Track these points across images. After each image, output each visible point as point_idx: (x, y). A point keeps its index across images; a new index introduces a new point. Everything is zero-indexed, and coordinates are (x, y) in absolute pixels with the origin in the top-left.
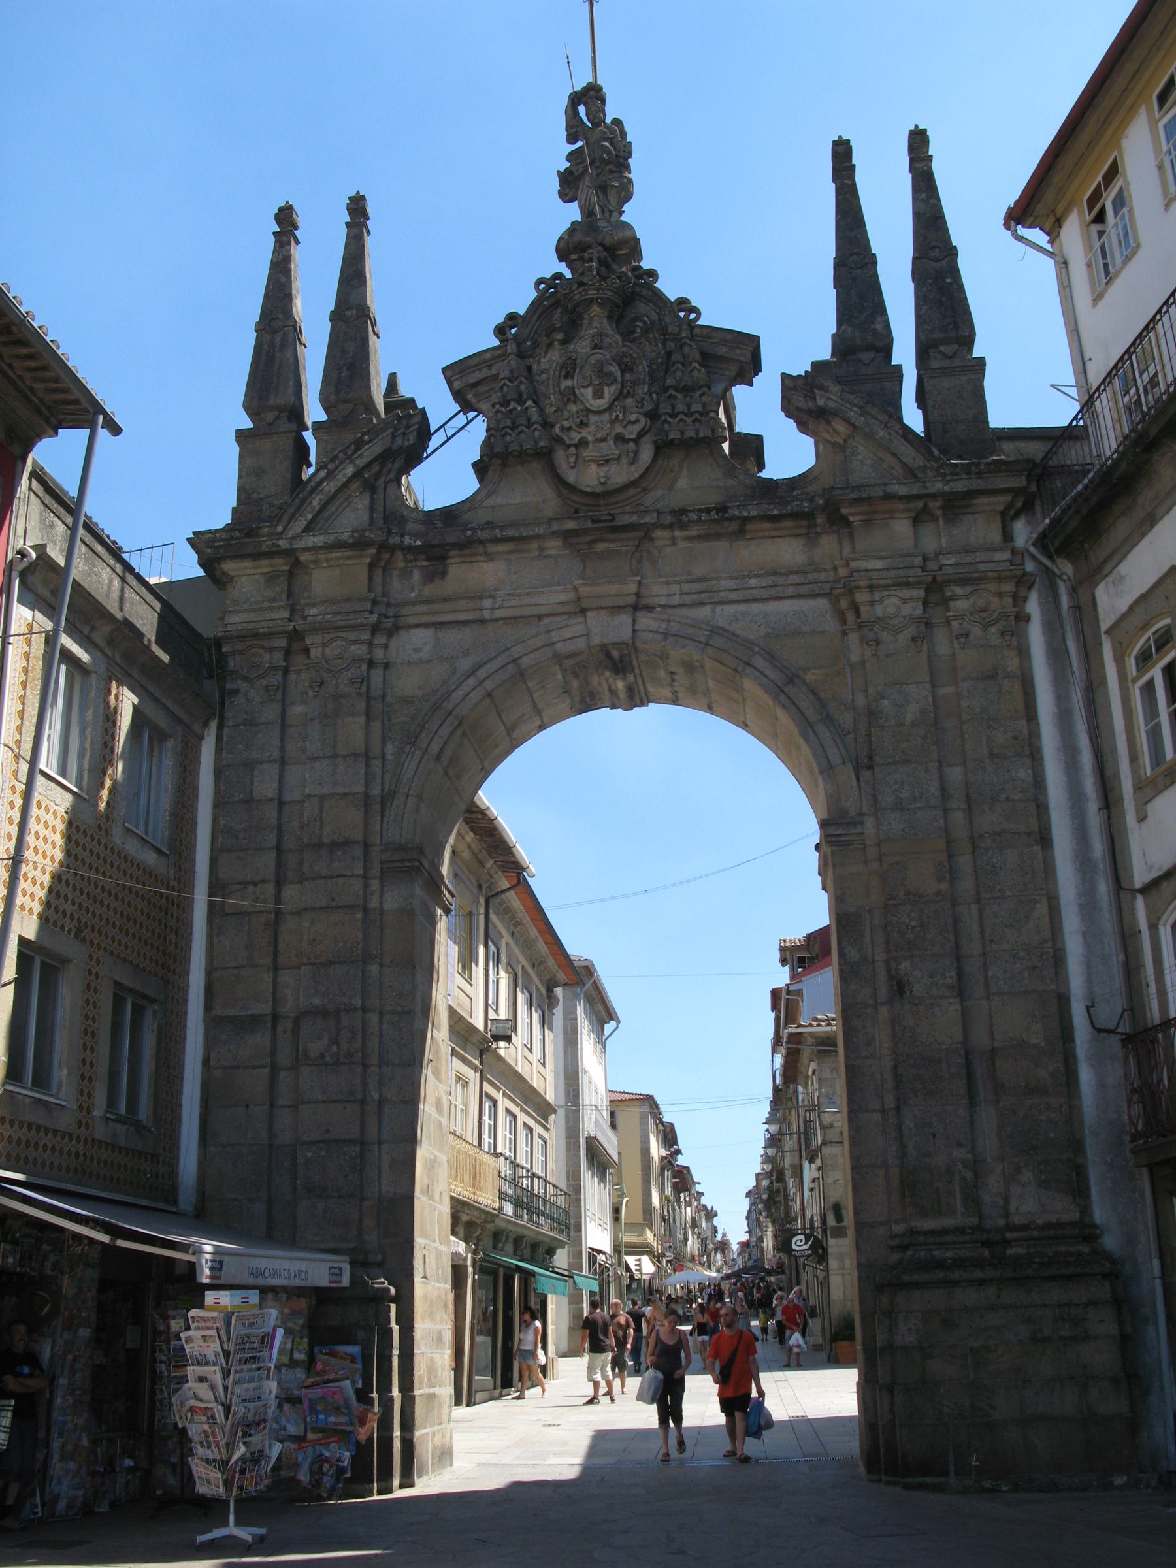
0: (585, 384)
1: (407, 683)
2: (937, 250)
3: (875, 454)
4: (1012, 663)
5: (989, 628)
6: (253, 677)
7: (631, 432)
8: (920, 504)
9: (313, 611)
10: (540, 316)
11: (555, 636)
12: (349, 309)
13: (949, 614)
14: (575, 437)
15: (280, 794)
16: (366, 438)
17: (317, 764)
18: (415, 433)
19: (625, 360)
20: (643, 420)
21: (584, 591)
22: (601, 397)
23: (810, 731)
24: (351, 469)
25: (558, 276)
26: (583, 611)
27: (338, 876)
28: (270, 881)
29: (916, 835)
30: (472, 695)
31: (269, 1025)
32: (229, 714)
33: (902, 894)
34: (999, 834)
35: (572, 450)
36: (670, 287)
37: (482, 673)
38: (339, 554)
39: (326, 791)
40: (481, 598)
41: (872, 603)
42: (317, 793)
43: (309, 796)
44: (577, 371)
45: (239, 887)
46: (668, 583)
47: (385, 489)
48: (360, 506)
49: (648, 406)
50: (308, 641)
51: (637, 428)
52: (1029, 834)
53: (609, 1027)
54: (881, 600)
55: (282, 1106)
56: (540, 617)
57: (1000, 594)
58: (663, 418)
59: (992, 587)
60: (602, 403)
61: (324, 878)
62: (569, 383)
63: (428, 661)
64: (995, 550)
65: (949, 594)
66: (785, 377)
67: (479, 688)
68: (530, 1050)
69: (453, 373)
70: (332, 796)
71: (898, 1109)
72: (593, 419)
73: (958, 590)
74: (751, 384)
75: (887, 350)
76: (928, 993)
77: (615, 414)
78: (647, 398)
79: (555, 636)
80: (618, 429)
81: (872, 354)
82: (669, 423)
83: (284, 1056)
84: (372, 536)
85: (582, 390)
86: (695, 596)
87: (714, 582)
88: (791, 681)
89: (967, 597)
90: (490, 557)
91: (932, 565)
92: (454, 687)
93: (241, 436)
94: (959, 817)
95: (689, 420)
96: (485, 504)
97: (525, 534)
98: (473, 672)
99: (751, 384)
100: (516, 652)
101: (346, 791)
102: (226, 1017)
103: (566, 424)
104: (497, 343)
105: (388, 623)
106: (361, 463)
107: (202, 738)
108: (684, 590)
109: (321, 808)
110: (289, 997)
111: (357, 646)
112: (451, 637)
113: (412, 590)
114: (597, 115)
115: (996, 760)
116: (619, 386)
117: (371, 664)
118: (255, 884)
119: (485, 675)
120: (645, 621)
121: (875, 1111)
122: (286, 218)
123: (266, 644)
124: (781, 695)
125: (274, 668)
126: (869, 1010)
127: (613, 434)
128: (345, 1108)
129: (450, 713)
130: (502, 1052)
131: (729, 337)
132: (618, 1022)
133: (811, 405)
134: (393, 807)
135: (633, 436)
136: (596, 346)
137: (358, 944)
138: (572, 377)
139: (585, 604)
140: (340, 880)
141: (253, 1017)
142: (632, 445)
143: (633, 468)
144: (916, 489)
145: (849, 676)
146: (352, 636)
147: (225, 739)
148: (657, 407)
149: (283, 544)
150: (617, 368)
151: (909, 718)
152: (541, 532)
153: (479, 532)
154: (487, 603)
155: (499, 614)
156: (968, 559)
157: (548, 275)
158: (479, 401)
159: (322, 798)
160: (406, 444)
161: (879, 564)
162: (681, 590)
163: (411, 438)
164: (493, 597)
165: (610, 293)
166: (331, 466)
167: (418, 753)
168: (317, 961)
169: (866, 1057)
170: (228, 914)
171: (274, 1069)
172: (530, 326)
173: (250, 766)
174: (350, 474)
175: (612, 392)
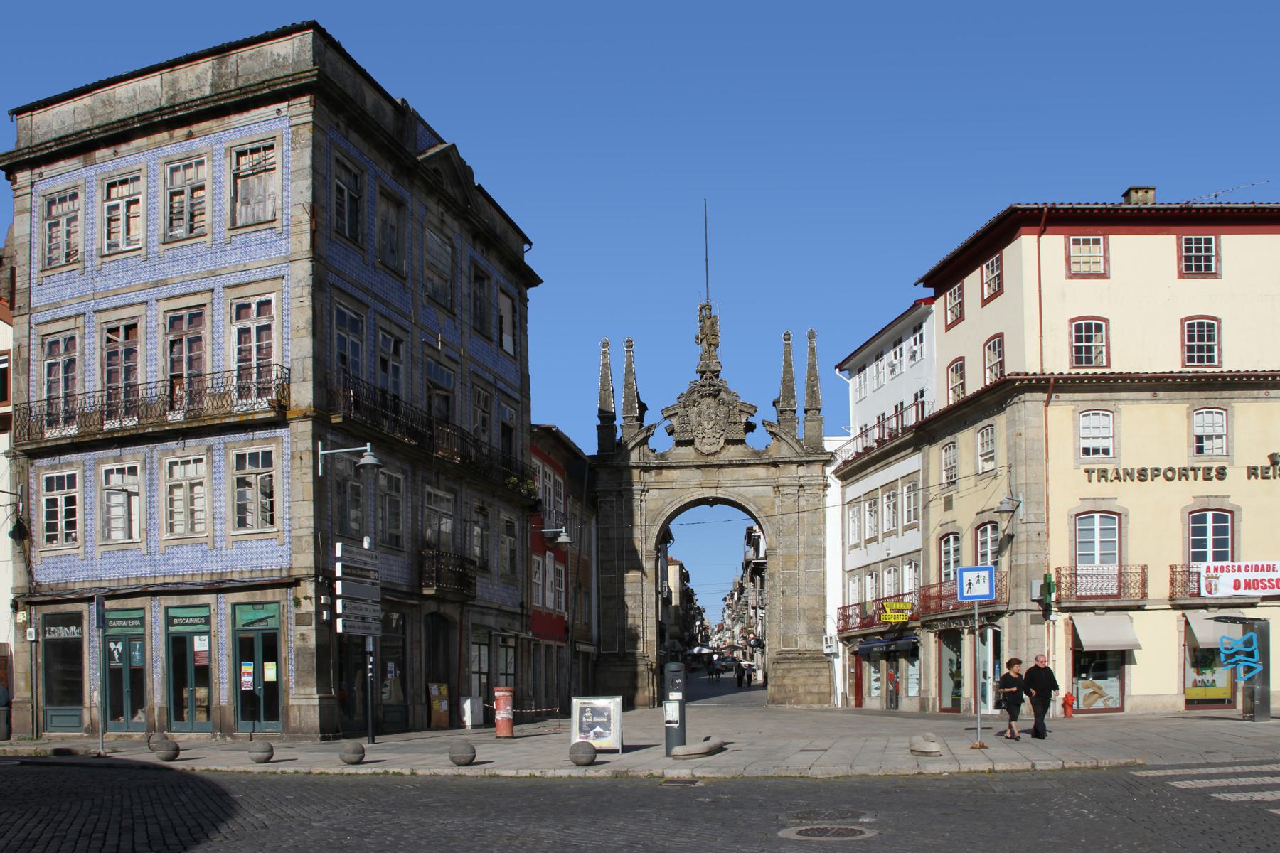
1: (651, 505)
7: (718, 435)
14: (701, 436)
37: (673, 504)
60: (710, 427)
72: (707, 431)
80: (714, 434)
88: (760, 510)
91: (801, 479)
93: (598, 426)
100: (682, 498)
105: (646, 489)
106: (637, 441)
112: (663, 492)
117: (641, 501)
120: (719, 491)
144: (798, 459)
157: (693, 380)
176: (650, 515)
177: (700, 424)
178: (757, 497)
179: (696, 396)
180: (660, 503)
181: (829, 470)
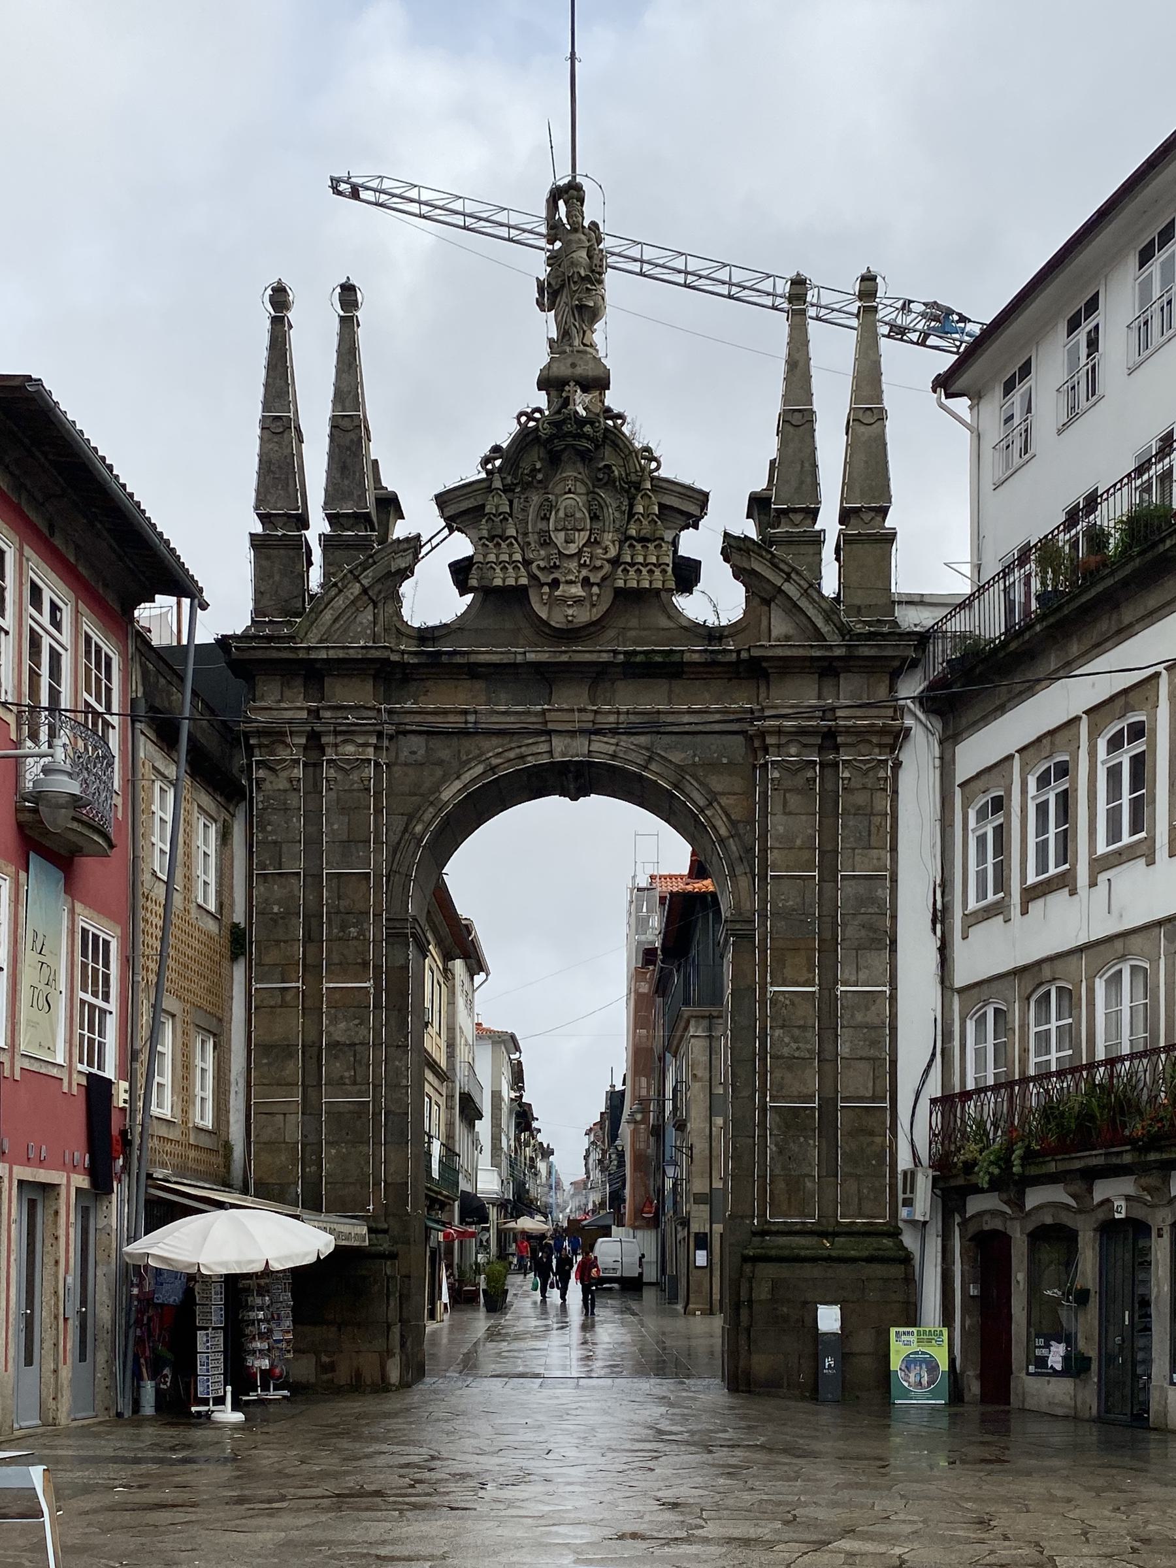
8: (826, 664)
20: (607, 567)
35: (546, 589)
51: (601, 574)
57: (880, 745)
59: (875, 740)
60: (573, 549)
69: (442, 500)
73: (849, 740)
75: (813, 514)
80: (584, 572)
103: (542, 564)
114: (575, 210)
116: (588, 533)
122: (280, 298)
127: (581, 578)
135: (598, 581)
138: (548, 519)
142: (595, 590)
148: (619, 555)
179: (535, 459)
181: (911, 687)
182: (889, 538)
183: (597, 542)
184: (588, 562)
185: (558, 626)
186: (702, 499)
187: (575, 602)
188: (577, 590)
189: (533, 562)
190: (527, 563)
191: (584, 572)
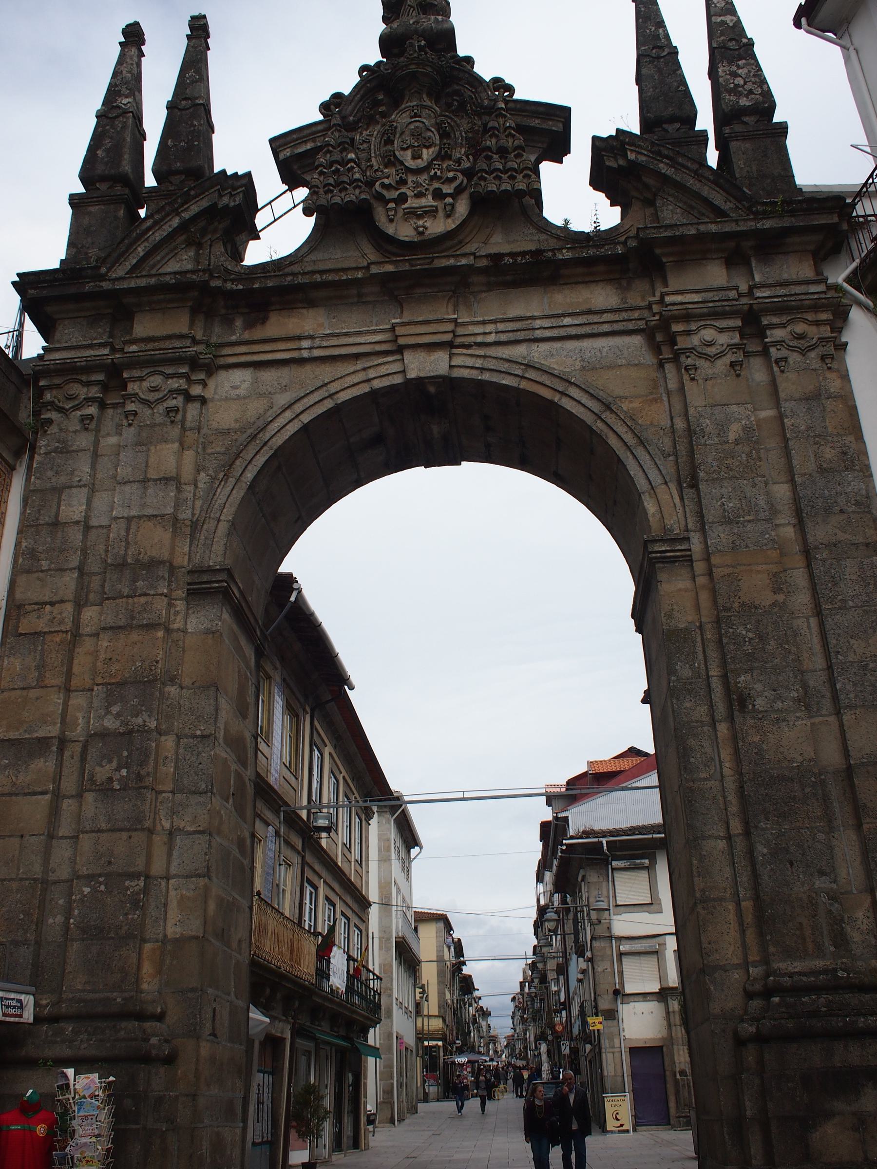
0: (405, 146)
2: (734, 42)
3: (685, 203)
4: (834, 384)
5: (809, 354)
6: (67, 407)
9: (134, 348)
10: (362, 97)
11: (372, 374)
12: (186, 99)
13: (766, 340)
14: (395, 194)
15: (87, 517)
16: (192, 193)
17: (127, 488)
18: (241, 195)
19: (443, 126)
20: (460, 176)
21: (399, 331)
22: (420, 157)
23: (629, 454)
24: (177, 221)
25: (381, 62)
26: (401, 350)
27: (140, 595)
28: (69, 601)
29: (747, 546)
30: (287, 427)
31: (54, 748)
32: (42, 443)
33: (736, 605)
34: (835, 545)
35: (392, 205)
36: (485, 70)
37: (298, 407)
38: (162, 297)
39: (134, 513)
40: (300, 338)
41: (688, 333)
42: (125, 515)
43: (116, 518)
44: (398, 135)
45: (36, 607)
46: (484, 323)
47: (211, 246)
48: (186, 257)
49: (466, 165)
50: (125, 375)
52: (867, 545)
53: (414, 851)
54: (698, 329)
55: (62, 838)
56: (357, 356)
57: (817, 323)
58: (479, 175)
59: (810, 317)
60: (420, 164)
61: (127, 597)
62: (389, 147)
63: (245, 398)
64: (808, 282)
65: (765, 322)
66: (595, 139)
67: (296, 421)
68: (349, 850)
69: (277, 144)
70: (140, 517)
71: (747, 833)
73: (775, 320)
74: (561, 162)
76: (771, 707)
77: (433, 172)
78: (464, 158)
79: (372, 374)
80: (436, 185)
81: (677, 125)
82: (485, 179)
83: (69, 785)
84: (194, 277)
85: (402, 153)
86: (511, 334)
87: (530, 321)
89: (783, 326)
90: (312, 304)
92: (271, 419)
94: (789, 532)
95: (505, 177)
96: (306, 259)
97: (345, 277)
98: (290, 406)
99: (561, 162)
100: (333, 387)
101: (155, 513)
102: (9, 740)
103: (386, 181)
104: (321, 117)
106: (186, 215)
107: (13, 468)
108: (500, 330)
109: (128, 530)
110: (80, 721)
111: (175, 379)
112: (269, 376)
113: (235, 334)
115: (825, 475)
116: (437, 148)
118: (52, 604)
119: (302, 409)
121: (718, 837)
123: (84, 378)
124: (599, 421)
125: (89, 400)
126: (706, 729)
127: (431, 189)
128: (130, 837)
129: (266, 443)
130: (324, 843)
131: (541, 109)
132: (421, 848)
133: (621, 162)
134: (204, 532)
135: (450, 191)
136: (416, 115)
137: (157, 662)
139: (402, 341)
140: (143, 600)
141: (39, 740)
142: (449, 200)
143: (450, 221)
145: (666, 404)
146: (169, 370)
147: (35, 466)
149: (106, 285)
150: (436, 133)
151: (732, 436)
152: (359, 276)
153: (300, 277)
154: (305, 344)
155: (317, 353)
156: (783, 291)
158: (303, 173)
159: (129, 519)
160: (232, 204)
161: (696, 298)
162: (497, 328)
163: (237, 199)
164: (311, 337)
165: (430, 69)
166: (157, 217)
167: (232, 481)
168: (113, 681)
169: (705, 779)
170: (21, 634)
171: (57, 796)
172: (353, 104)
173: (58, 491)
174: (176, 225)
175: (431, 153)
176: (218, 447)
177: (391, 161)
178: (594, 369)
180: (254, 408)
182: (783, 128)
183: (449, 157)
184: (439, 173)
185: (407, 239)
186: (562, 114)
187: (426, 212)
188: (428, 201)
189: (377, 181)
190: (370, 184)
191: (436, 185)
